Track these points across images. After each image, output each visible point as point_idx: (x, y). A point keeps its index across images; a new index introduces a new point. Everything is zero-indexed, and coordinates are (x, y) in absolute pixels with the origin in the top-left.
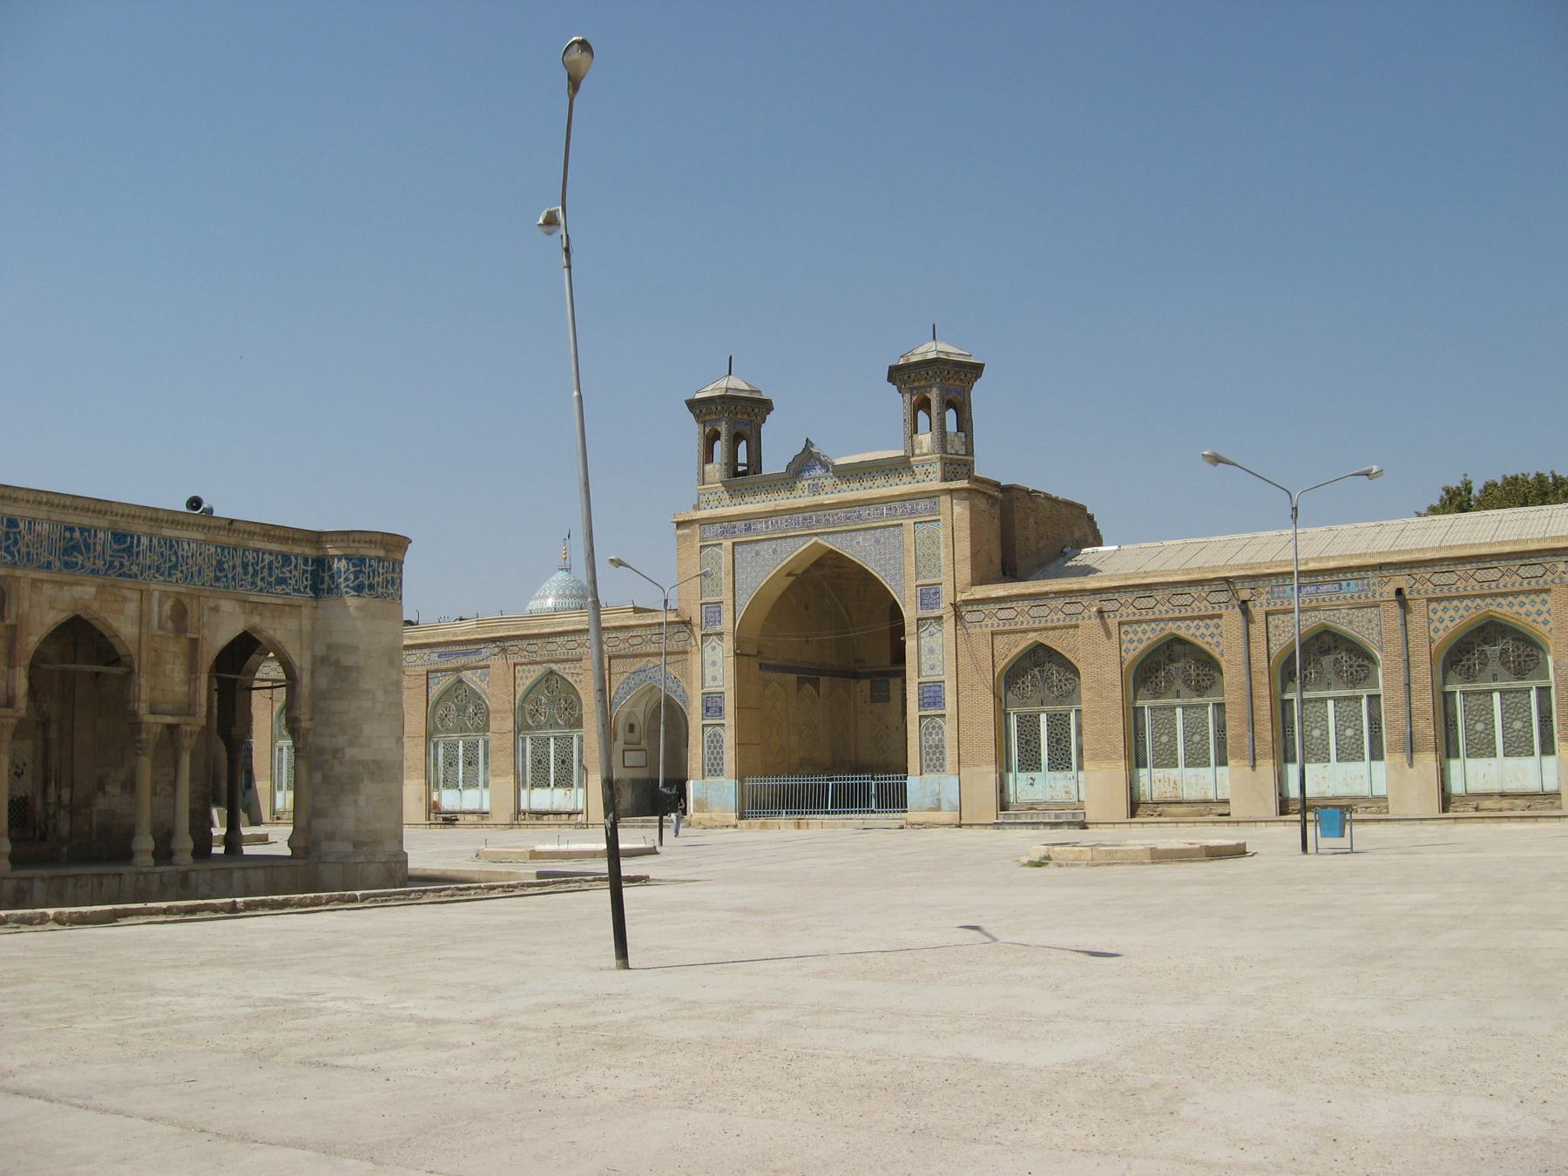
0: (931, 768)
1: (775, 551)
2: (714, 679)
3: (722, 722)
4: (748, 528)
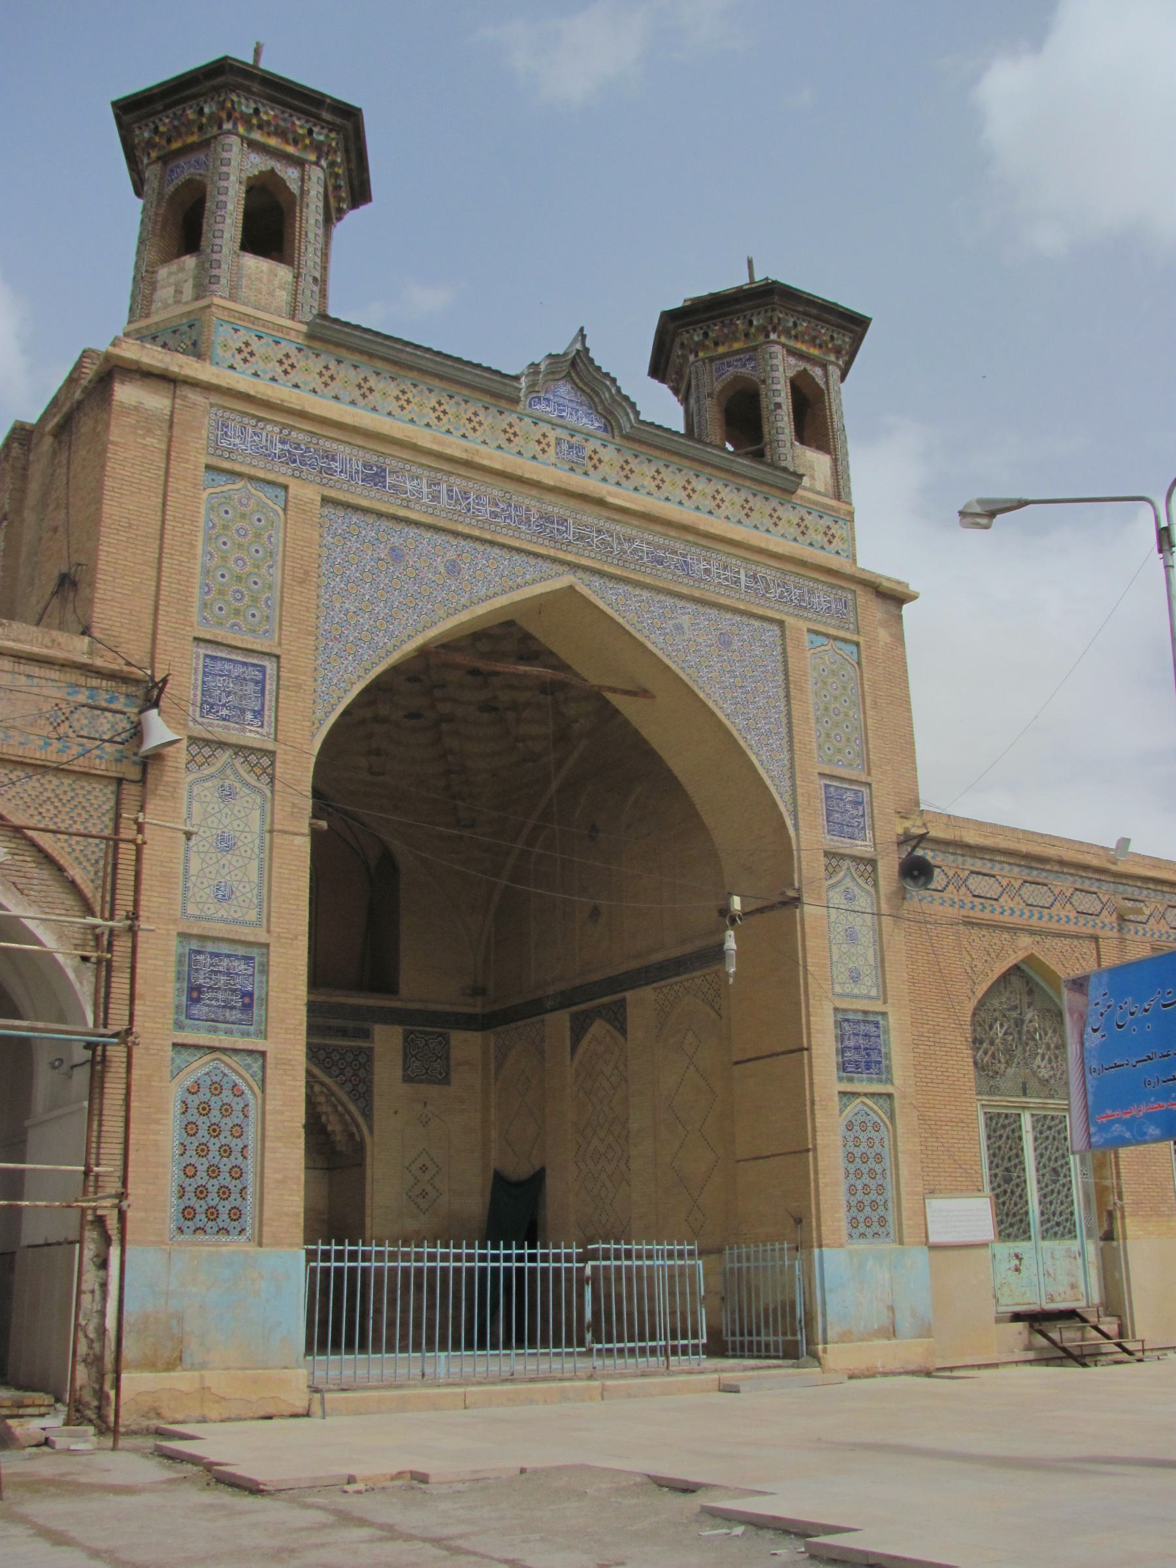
0: (862, 1228)
1: (453, 569)
2: (224, 895)
3: (259, 1044)
4: (376, 477)
